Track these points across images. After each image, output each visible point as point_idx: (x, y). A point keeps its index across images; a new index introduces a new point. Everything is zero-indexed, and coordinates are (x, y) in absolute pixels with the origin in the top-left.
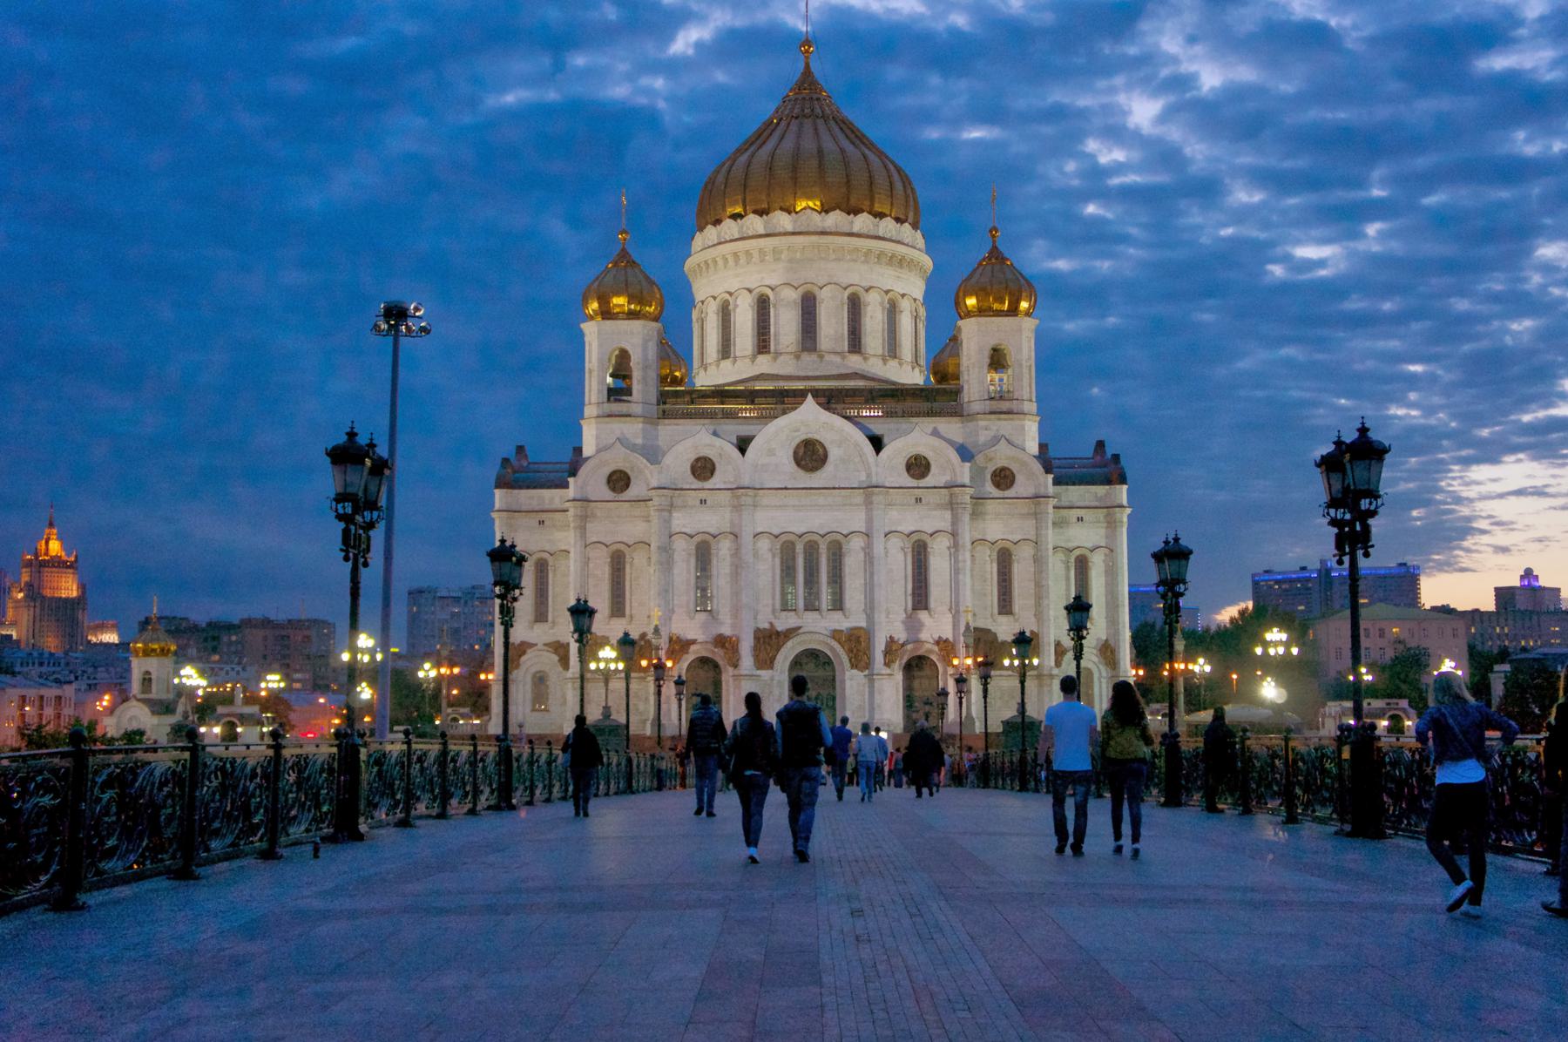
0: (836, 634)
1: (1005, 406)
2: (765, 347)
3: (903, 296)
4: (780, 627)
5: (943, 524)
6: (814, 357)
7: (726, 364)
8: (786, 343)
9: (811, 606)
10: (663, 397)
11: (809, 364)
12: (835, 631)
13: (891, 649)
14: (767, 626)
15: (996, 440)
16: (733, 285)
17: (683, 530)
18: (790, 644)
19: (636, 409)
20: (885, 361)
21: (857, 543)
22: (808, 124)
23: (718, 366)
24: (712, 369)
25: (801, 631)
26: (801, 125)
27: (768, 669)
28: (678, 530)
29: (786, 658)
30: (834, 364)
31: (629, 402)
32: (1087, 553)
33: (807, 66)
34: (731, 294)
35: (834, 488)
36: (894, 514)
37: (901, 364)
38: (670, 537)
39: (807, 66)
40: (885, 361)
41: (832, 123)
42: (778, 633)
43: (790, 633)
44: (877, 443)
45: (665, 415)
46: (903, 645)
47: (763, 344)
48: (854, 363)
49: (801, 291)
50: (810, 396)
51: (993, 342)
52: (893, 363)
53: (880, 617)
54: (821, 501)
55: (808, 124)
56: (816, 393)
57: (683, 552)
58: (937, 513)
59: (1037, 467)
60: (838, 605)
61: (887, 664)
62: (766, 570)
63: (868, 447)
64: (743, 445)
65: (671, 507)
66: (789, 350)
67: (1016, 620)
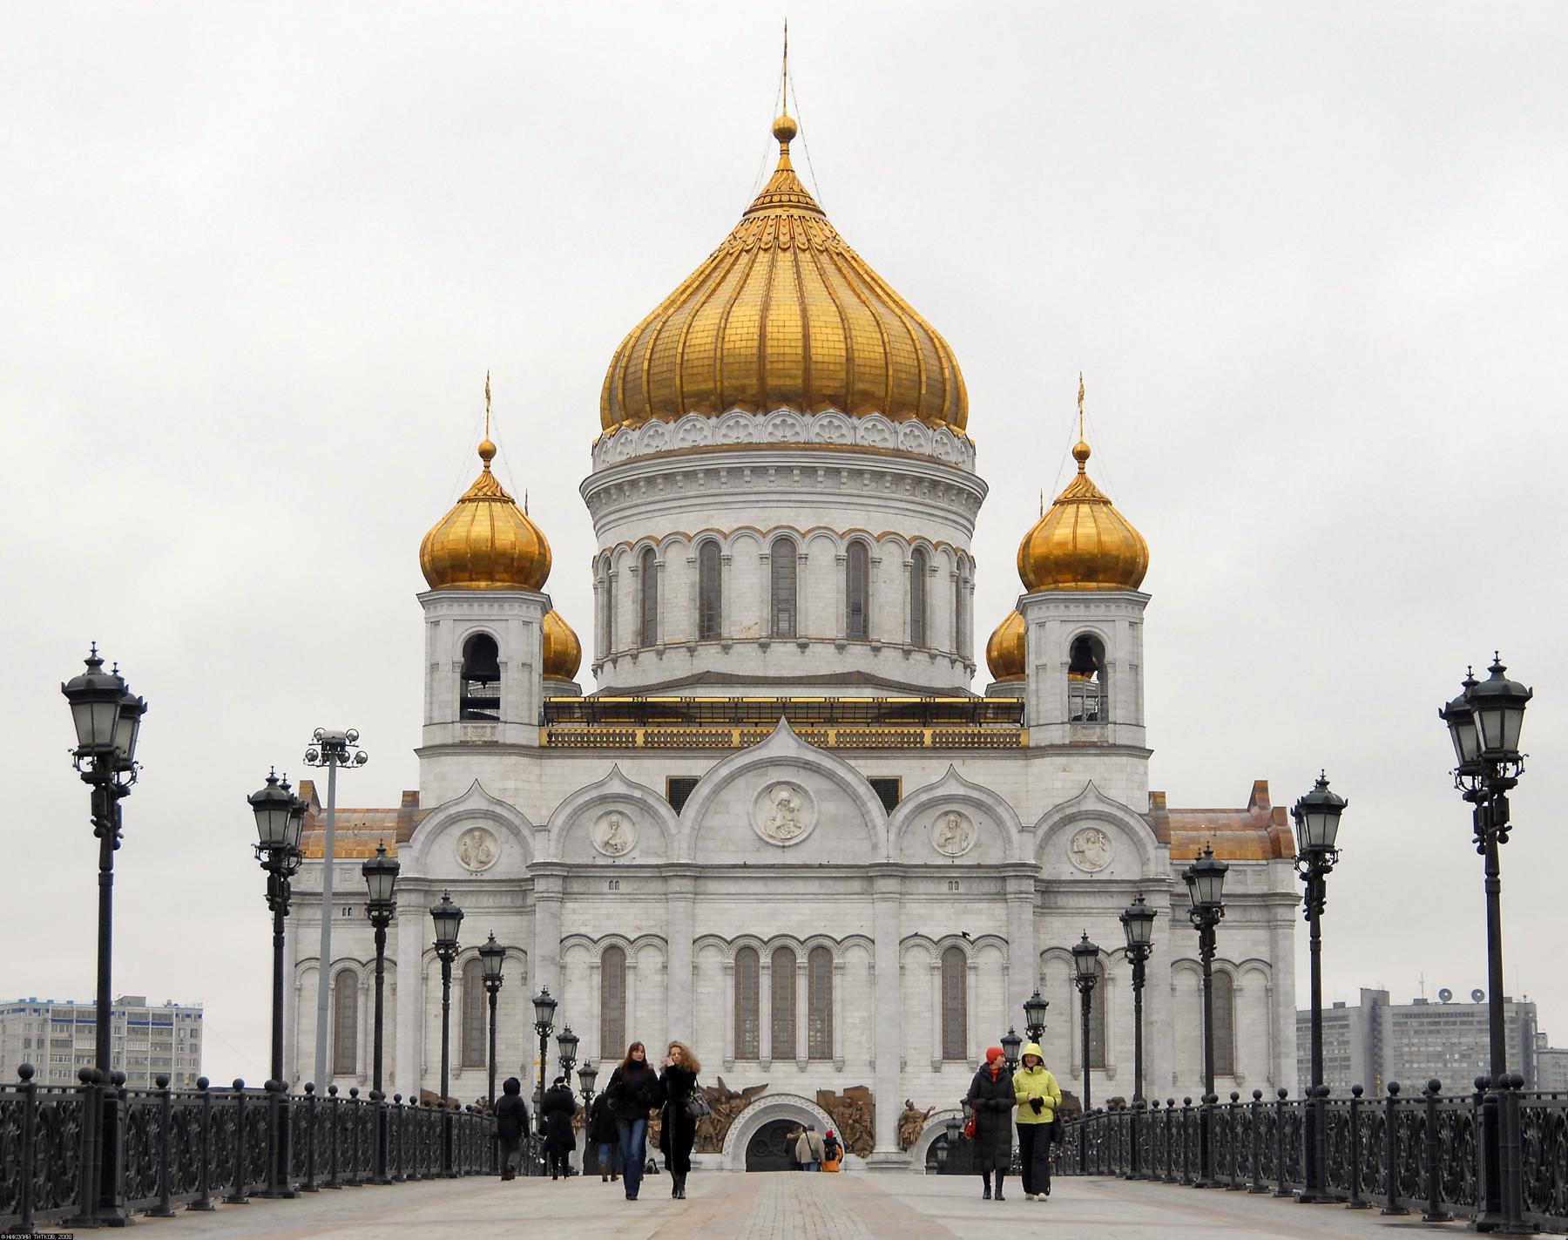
0: (825, 1099)
1: (1094, 734)
2: (710, 629)
3: (936, 546)
4: (735, 1085)
5: (991, 923)
6: (791, 647)
7: (648, 658)
8: (746, 623)
9: (783, 1051)
10: (552, 713)
11: (784, 660)
12: (820, 1093)
13: (910, 1119)
14: (714, 1084)
15: (1088, 788)
16: (660, 526)
17: (583, 930)
18: (748, 1112)
19: (508, 734)
20: (907, 653)
21: (854, 958)
22: (785, 259)
23: (635, 657)
24: (625, 663)
25: (766, 1093)
26: (773, 264)
27: (715, 1151)
28: (574, 931)
29: (742, 1134)
30: (823, 661)
31: (497, 719)
32: (1229, 967)
33: (785, 170)
34: (658, 542)
35: (821, 866)
36: (915, 908)
37: (933, 657)
38: (561, 941)
39: (785, 170)
40: (907, 653)
41: (824, 258)
42: (732, 1096)
43: (750, 1094)
44: (888, 791)
45: (552, 748)
46: (926, 1117)
47: (709, 624)
48: (857, 659)
49: (771, 537)
50: (783, 720)
51: (1078, 629)
52: (919, 658)
53: (887, 1067)
54: (800, 887)
55: (785, 259)
56: (796, 713)
57: (583, 961)
58: (984, 905)
59: (1144, 832)
60: (823, 1050)
61: (905, 1143)
62: (718, 992)
63: (874, 805)
64: (679, 791)
65: (566, 895)
66: (754, 633)
67: (1110, 1078)
